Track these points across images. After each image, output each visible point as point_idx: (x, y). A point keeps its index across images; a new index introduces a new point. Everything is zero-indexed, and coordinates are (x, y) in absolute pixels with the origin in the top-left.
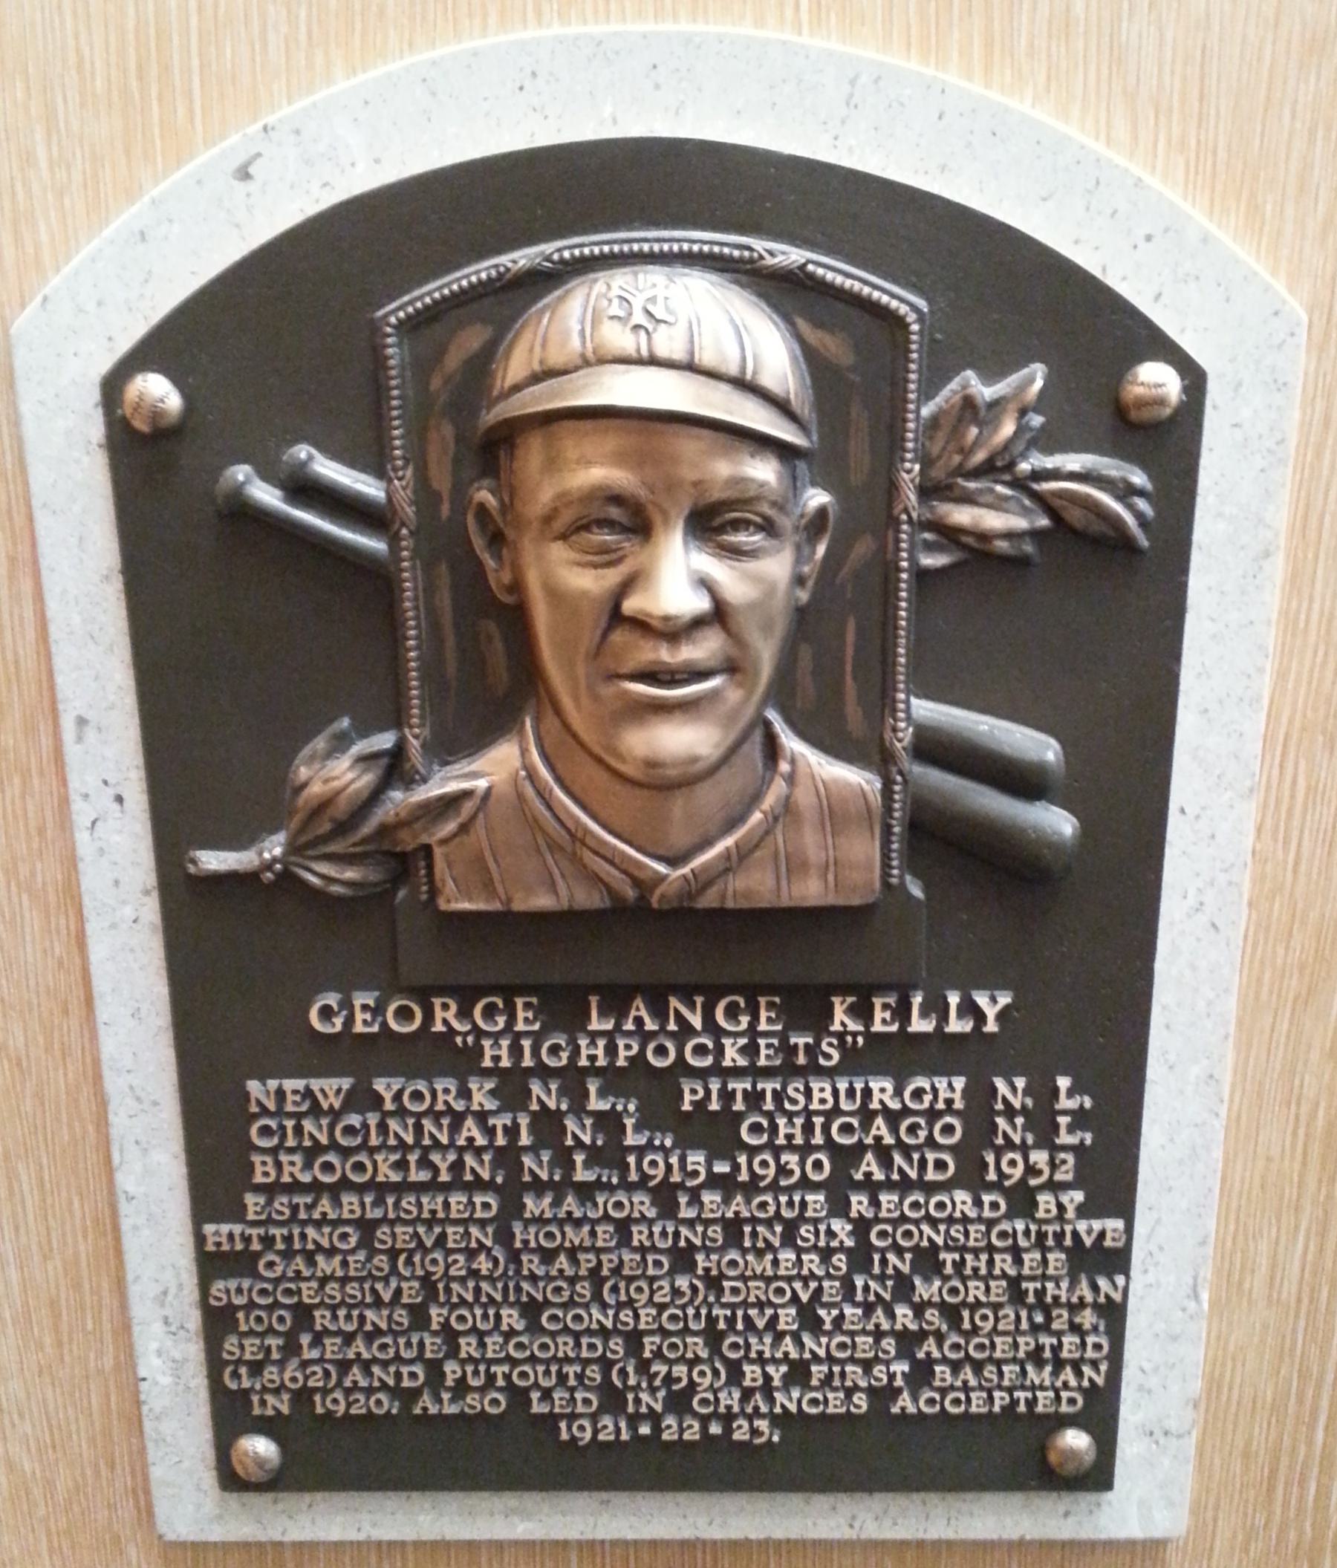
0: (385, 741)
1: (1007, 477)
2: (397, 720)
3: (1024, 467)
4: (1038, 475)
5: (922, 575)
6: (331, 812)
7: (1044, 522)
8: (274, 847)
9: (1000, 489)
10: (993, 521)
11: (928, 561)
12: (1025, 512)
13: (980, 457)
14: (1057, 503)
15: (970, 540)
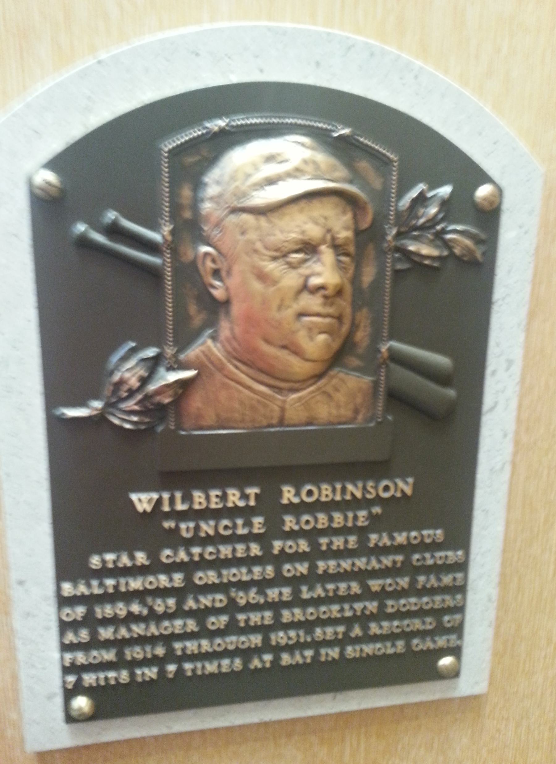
0: (151, 352)
1: (433, 231)
2: (158, 344)
3: (439, 227)
4: (444, 231)
5: (396, 272)
6: (126, 387)
7: (445, 253)
8: (97, 404)
9: (429, 236)
10: (425, 250)
11: (399, 266)
12: (437, 247)
13: (422, 221)
14: (452, 244)
15: (416, 259)
